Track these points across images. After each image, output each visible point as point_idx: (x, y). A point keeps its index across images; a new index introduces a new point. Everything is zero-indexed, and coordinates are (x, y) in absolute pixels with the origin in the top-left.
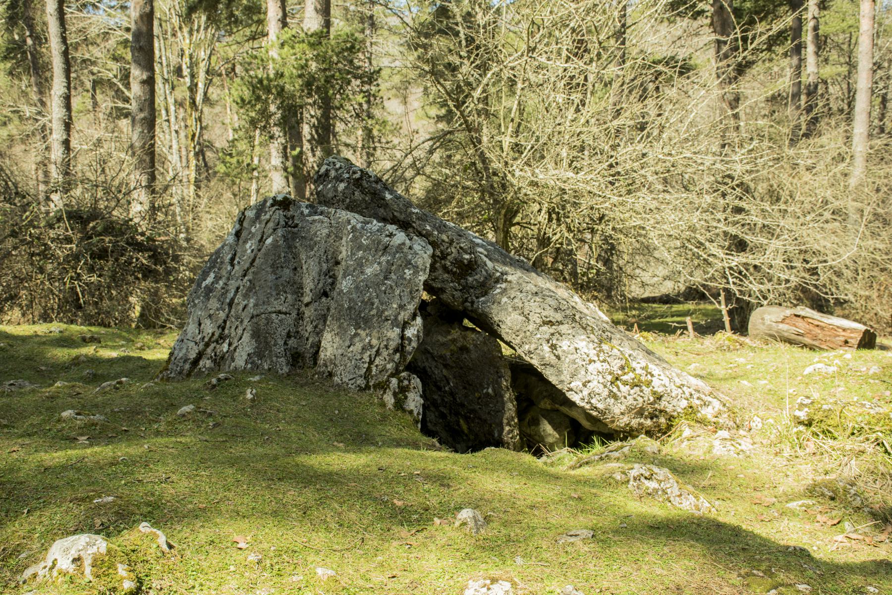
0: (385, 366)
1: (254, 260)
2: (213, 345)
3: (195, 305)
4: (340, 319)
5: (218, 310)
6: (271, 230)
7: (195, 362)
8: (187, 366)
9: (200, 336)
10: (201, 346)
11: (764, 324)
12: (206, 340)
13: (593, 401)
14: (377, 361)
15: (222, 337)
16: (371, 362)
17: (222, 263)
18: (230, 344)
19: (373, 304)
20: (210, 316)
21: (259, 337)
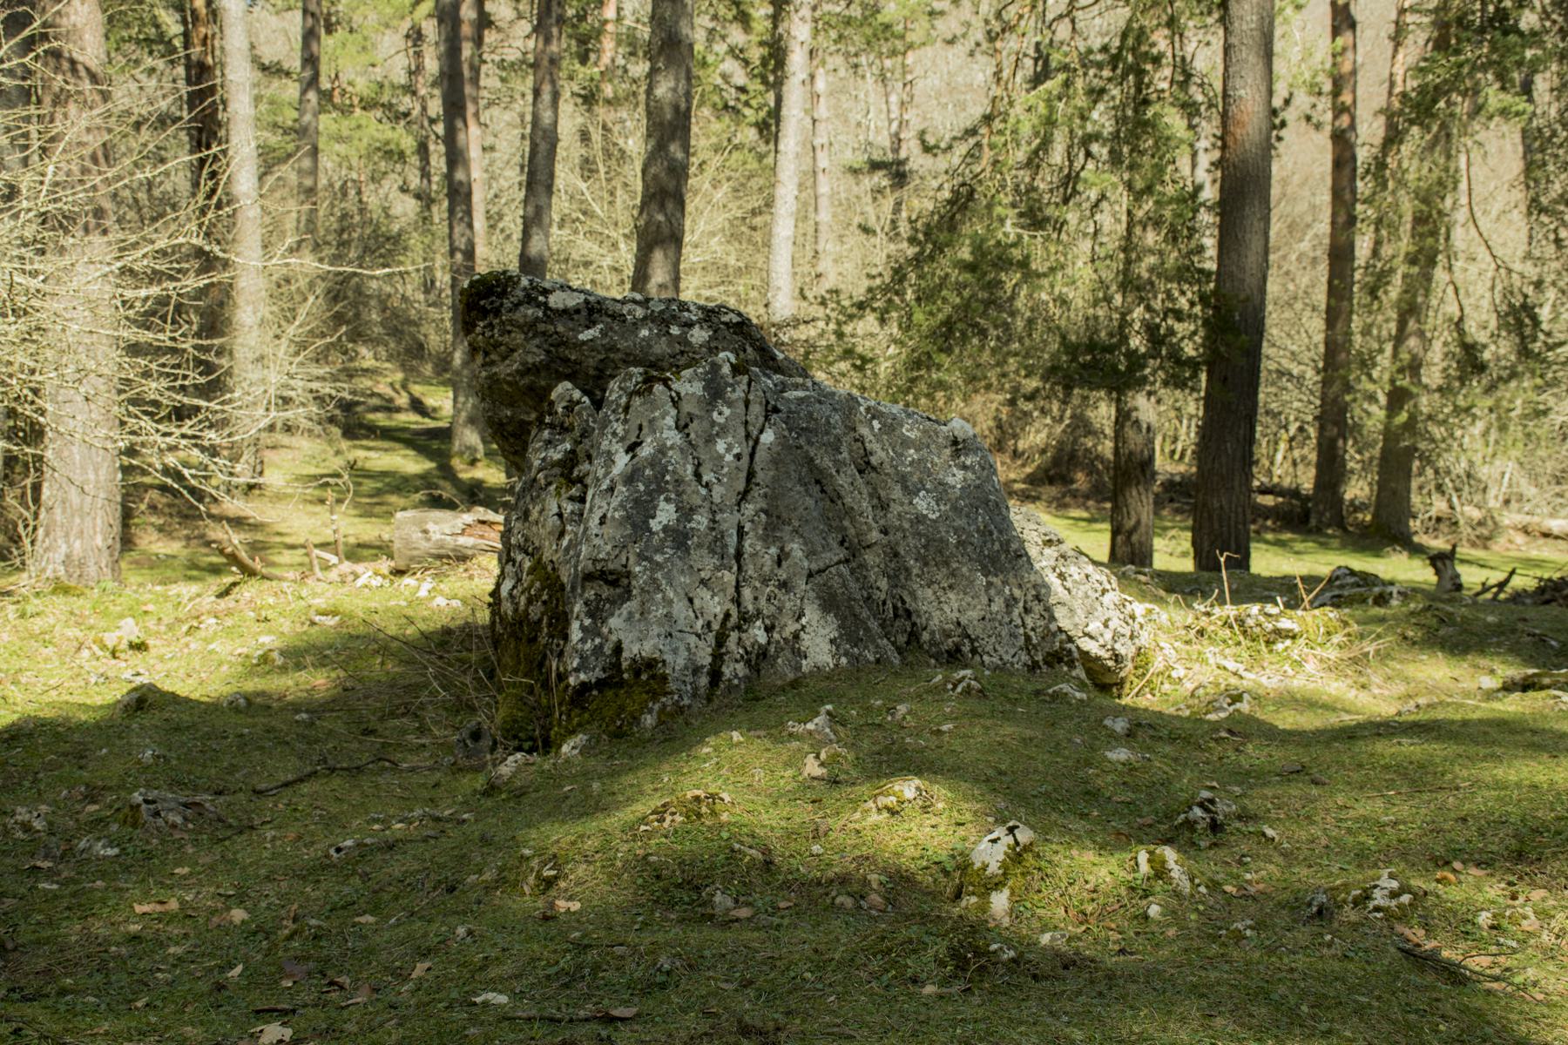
0: (1047, 627)
1: (751, 475)
2: (734, 635)
3: (659, 566)
4: (947, 564)
5: (718, 569)
6: (762, 419)
7: (715, 675)
8: (704, 681)
9: (700, 623)
10: (711, 637)
11: (429, 540)
12: (716, 626)
13: (1117, 646)
14: (1029, 621)
15: (745, 619)
16: (1024, 625)
17: (678, 482)
18: (769, 629)
19: (991, 533)
20: (703, 582)
21: (838, 608)
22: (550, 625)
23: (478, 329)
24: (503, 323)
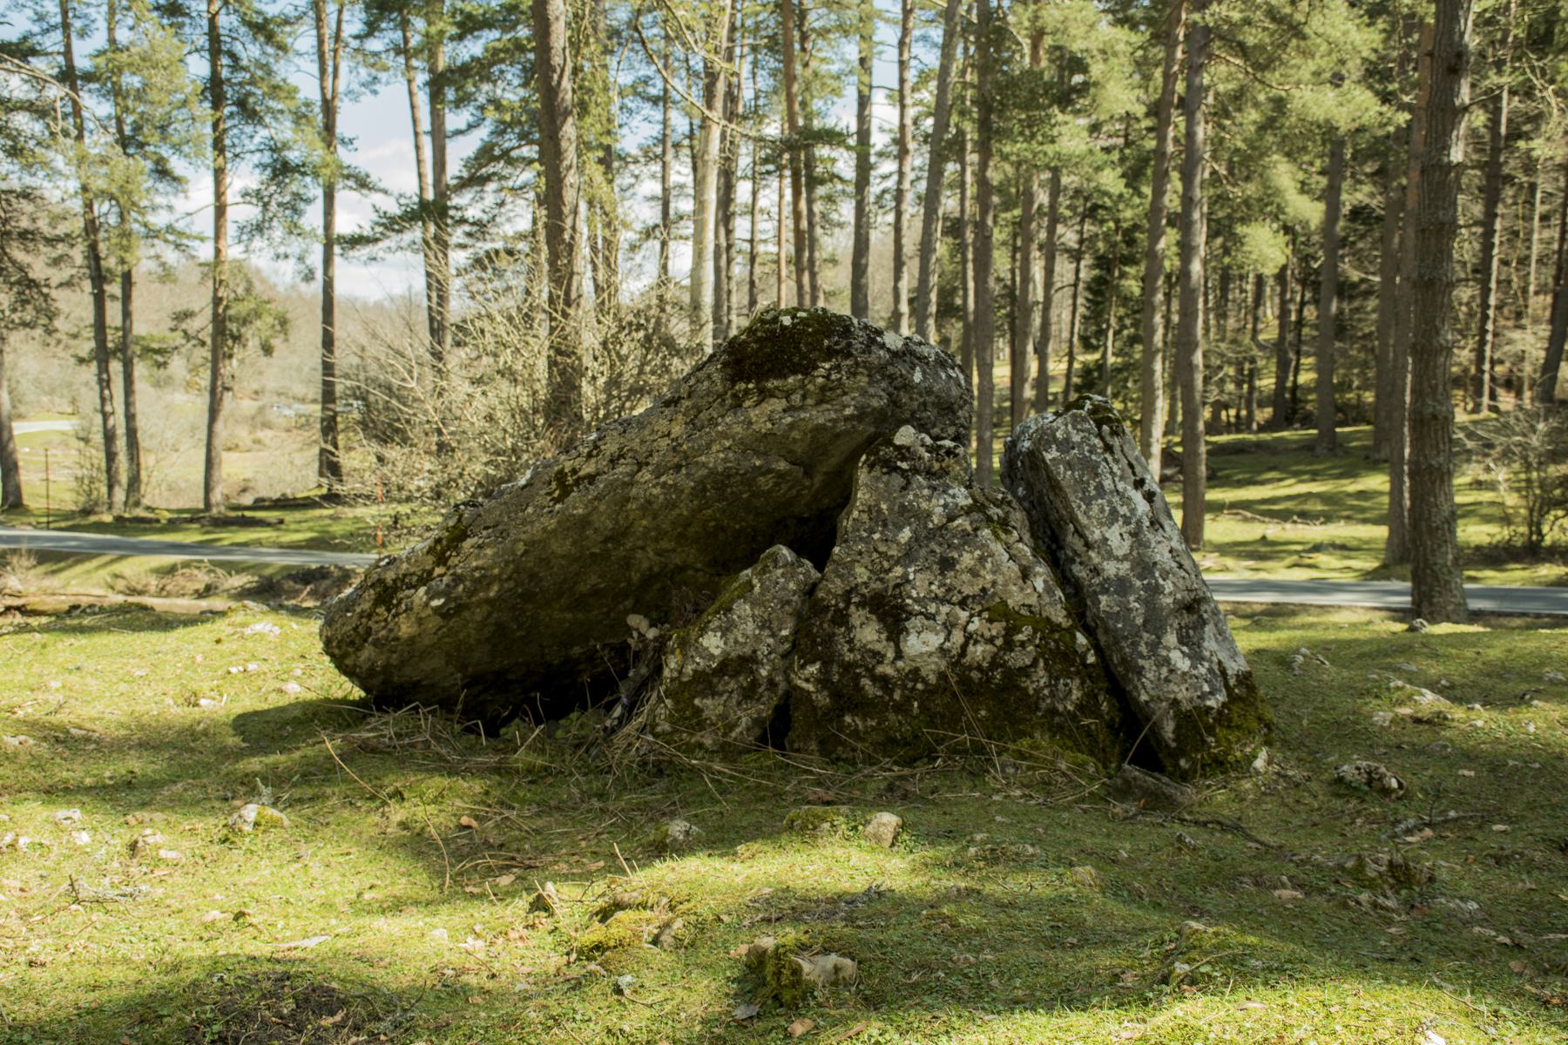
22: (1047, 668)
24: (857, 364)
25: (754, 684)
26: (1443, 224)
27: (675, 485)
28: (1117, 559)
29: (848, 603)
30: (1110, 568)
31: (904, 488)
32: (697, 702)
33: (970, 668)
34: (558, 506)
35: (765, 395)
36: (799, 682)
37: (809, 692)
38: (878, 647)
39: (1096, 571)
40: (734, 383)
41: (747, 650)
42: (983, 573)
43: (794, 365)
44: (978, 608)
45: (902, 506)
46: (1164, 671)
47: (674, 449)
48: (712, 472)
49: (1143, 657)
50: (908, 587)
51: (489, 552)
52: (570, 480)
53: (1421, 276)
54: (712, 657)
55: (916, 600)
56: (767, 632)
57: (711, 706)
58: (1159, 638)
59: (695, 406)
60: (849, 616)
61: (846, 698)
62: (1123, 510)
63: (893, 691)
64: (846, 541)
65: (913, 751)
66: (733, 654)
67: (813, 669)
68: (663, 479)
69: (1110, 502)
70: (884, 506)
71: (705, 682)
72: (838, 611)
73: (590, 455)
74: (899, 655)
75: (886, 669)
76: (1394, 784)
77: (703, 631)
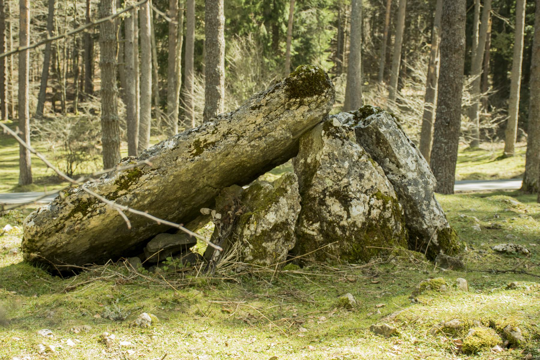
23: (324, 94)
25: (289, 235)
26: (112, 40)
27: (259, 146)
28: (412, 171)
29: (325, 196)
30: (411, 175)
31: (343, 145)
32: (264, 245)
33: (372, 220)
34: (197, 158)
35: (301, 104)
36: (309, 232)
37: (313, 235)
38: (340, 213)
39: (404, 176)
40: (290, 98)
41: (284, 219)
42: (372, 179)
43: (316, 90)
44: (371, 194)
45: (344, 152)
46: (432, 215)
47: (259, 129)
48: (276, 140)
49: (425, 210)
50: (350, 187)
51: (155, 181)
52: (202, 145)
53: (104, 61)
54: (270, 223)
55: (353, 193)
56: (292, 211)
57: (270, 246)
58: (429, 202)
59: (269, 109)
60: (325, 201)
61: (328, 236)
62: (410, 151)
63: (346, 232)
64: (321, 168)
65: (358, 256)
66: (279, 222)
67: (317, 225)
68: (253, 143)
69: (406, 148)
70: (336, 153)
71: (267, 235)
72: (321, 199)
73: (213, 133)
74: (349, 216)
75: (344, 223)
76: (527, 251)
77: (267, 212)
